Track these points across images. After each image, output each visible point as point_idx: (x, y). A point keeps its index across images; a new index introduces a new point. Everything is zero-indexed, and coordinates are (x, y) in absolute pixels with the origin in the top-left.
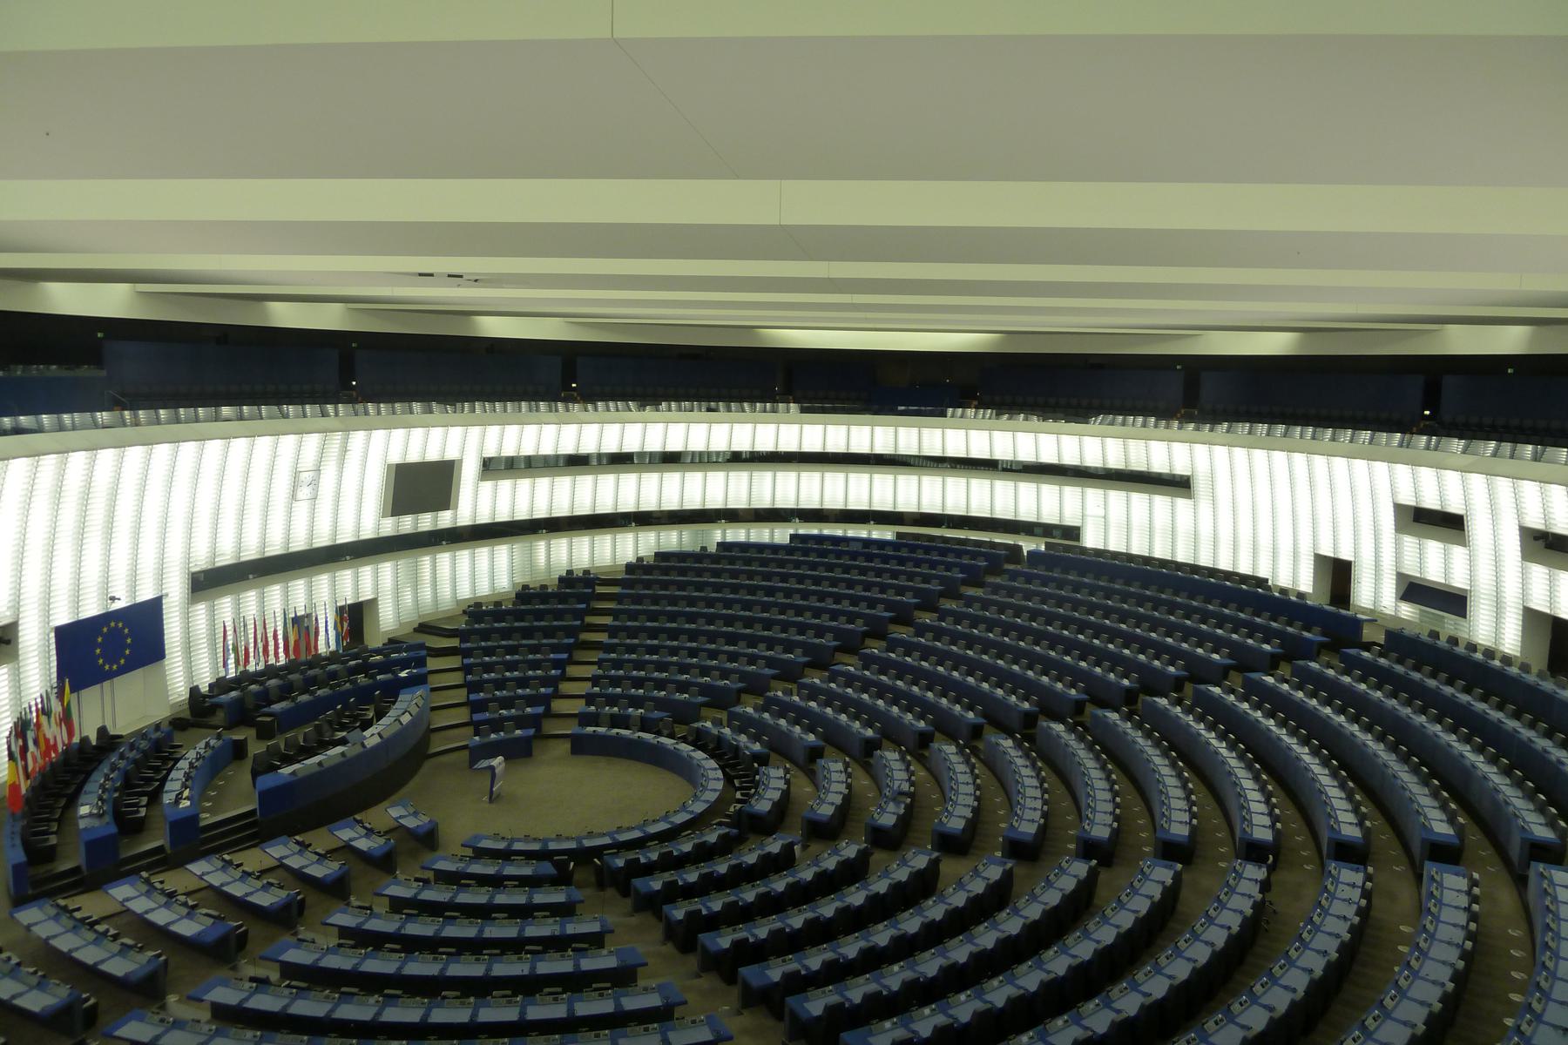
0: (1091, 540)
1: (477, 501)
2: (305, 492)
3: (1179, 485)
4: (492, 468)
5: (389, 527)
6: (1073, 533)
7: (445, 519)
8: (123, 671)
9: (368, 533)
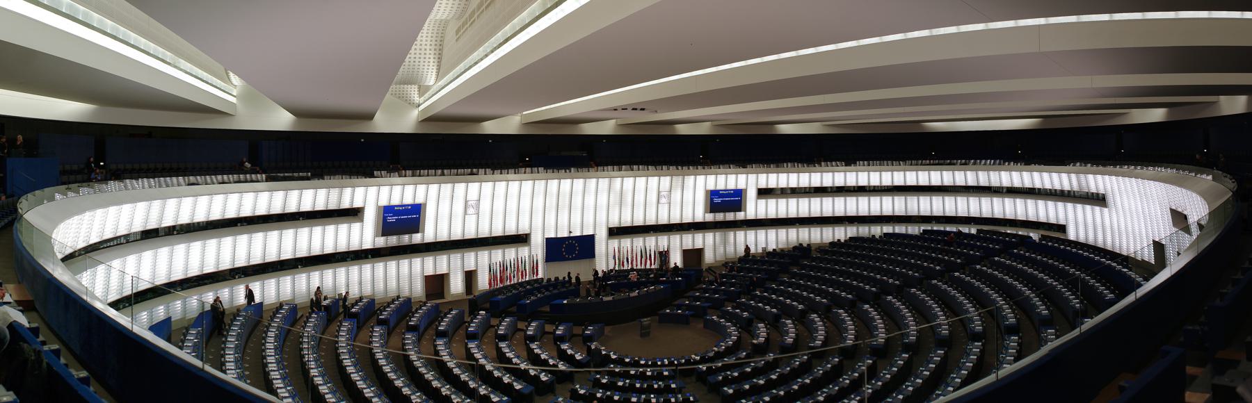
0: (1072, 235)
1: (755, 208)
2: (663, 200)
3: (1099, 200)
4: (764, 193)
5: (710, 217)
6: (1062, 228)
7: (740, 216)
8: (573, 259)
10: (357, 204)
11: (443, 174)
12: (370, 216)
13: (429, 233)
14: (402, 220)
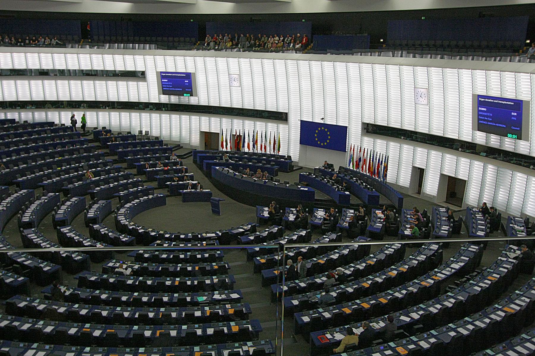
8: (324, 147)
9: (467, 137)
10: (140, 68)
11: (133, 48)
12: (152, 78)
13: (202, 98)
14: (178, 83)
